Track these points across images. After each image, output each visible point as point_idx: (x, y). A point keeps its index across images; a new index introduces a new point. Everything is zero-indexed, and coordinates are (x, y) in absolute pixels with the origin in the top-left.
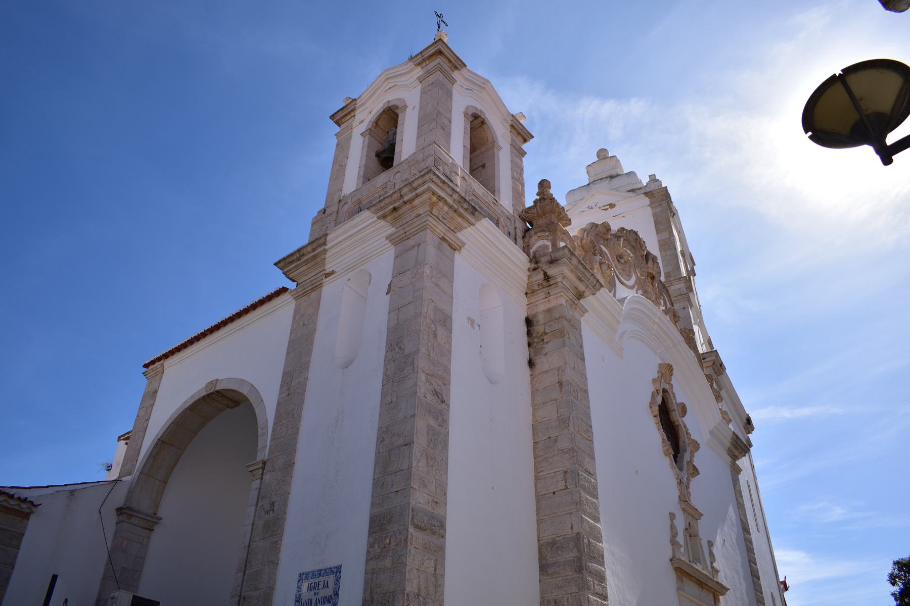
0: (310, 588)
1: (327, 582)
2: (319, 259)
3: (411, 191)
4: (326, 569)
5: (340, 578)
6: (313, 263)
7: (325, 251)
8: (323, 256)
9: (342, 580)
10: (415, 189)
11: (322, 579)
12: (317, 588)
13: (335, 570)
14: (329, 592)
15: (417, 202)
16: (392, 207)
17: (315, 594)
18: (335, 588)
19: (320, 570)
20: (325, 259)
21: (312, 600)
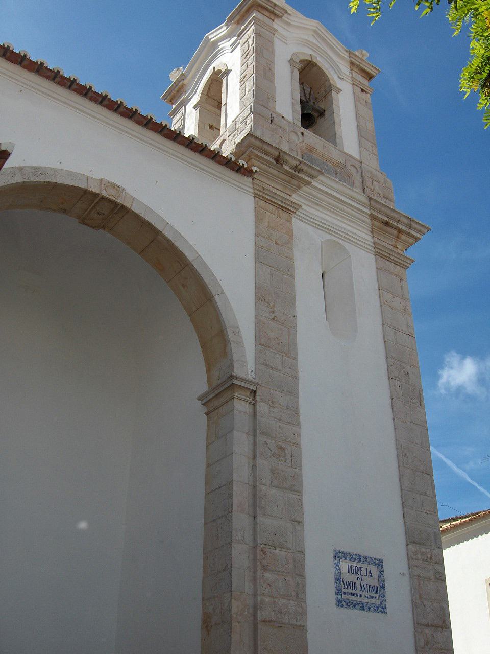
0: (351, 570)
1: (370, 572)
2: (295, 182)
3: (407, 225)
4: (366, 558)
5: (383, 571)
6: (287, 178)
7: (309, 183)
8: (302, 185)
9: (385, 574)
10: (410, 227)
11: (364, 566)
12: (359, 573)
13: (377, 562)
14: (374, 581)
15: (403, 237)
16: (387, 219)
17: (358, 579)
18: (380, 581)
19: (360, 556)
20: (299, 187)
21: (355, 584)
